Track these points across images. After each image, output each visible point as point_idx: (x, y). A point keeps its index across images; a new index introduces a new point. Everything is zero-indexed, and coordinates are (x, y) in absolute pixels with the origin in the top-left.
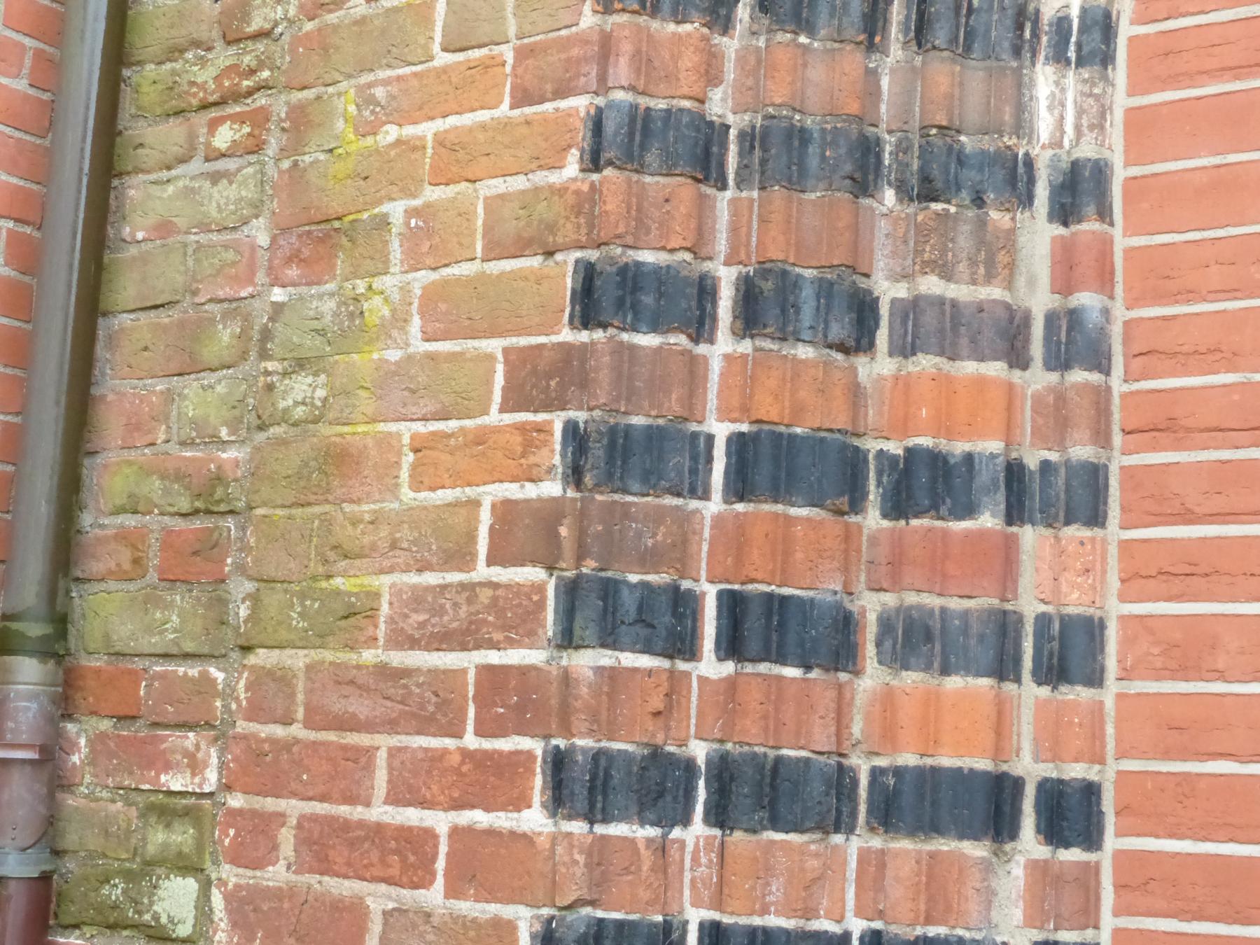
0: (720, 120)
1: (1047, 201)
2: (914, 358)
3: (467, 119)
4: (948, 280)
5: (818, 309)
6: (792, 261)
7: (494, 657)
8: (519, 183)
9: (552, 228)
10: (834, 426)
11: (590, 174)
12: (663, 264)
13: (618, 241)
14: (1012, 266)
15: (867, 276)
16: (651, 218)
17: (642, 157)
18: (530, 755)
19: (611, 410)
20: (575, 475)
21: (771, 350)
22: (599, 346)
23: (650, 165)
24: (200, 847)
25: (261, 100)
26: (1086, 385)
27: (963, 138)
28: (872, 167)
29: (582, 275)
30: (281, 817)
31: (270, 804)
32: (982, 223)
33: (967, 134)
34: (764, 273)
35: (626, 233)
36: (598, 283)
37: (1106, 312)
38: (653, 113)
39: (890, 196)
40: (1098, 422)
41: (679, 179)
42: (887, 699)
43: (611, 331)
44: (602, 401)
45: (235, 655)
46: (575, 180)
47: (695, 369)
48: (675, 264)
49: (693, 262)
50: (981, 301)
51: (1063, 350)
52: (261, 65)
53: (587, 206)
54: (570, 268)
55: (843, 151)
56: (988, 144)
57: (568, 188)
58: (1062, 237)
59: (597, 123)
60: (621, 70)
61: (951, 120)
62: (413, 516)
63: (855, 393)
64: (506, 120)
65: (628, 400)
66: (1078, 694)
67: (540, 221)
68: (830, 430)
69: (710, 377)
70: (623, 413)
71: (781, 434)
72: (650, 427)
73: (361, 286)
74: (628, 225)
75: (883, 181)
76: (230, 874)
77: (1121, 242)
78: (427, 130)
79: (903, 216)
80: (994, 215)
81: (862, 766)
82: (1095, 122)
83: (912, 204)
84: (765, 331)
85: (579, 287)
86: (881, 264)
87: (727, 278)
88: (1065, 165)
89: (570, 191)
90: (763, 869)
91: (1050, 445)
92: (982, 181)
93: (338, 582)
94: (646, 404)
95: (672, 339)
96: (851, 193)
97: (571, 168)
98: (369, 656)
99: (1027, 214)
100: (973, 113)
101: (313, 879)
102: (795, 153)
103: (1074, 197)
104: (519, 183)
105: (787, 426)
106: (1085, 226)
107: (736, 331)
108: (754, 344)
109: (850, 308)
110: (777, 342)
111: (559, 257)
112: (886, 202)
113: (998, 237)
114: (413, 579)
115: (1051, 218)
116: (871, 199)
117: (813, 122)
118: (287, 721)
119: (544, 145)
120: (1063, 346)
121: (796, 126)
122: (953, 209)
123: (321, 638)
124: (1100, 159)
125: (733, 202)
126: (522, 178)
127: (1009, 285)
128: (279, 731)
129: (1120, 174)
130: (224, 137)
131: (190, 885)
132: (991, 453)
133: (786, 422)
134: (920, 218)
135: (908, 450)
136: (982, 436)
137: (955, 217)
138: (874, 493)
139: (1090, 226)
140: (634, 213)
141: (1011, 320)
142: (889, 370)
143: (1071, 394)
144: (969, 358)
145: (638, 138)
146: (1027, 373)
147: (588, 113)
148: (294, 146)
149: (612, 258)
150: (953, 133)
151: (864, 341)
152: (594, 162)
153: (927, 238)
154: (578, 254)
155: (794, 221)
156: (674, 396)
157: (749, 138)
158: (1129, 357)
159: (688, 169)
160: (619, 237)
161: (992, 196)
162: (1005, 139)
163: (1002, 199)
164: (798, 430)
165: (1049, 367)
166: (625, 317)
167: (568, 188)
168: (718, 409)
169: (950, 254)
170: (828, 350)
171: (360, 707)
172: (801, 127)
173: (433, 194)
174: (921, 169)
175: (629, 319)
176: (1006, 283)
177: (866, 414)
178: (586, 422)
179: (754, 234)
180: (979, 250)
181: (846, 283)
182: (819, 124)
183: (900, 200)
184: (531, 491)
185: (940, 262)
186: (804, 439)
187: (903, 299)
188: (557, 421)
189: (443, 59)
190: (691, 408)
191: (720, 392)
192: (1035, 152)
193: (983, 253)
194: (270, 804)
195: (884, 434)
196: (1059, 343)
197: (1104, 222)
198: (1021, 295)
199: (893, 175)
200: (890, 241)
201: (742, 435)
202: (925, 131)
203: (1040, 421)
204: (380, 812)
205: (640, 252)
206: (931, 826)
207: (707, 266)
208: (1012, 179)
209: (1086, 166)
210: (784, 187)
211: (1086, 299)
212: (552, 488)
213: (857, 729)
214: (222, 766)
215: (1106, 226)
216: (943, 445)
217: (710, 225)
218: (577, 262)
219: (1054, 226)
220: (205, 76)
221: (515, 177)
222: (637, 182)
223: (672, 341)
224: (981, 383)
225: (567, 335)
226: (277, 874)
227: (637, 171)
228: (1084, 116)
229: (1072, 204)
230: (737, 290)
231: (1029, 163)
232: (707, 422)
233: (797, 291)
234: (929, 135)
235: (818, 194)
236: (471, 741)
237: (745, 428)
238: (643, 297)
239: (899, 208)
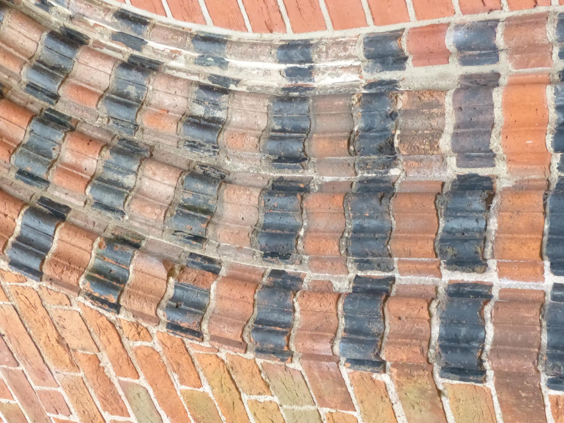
0: (352, 283)
1: (393, 72)
2: (494, 150)
4: (442, 132)
5: (465, 217)
6: (434, 236)
8: (398, 408)
9: (423, 392)
10: (542, 203)
11: (387, 367)
12: (440, 321)
13: (425, 352)
14: (431, 91)
15: (443, 184)
16: (412, 328)
17: (373, 335)
19: (538, 359)
21: (492, 248)
22: (494, 366)
23: (379, 330)
26: (505, 34)
27: (356, 129)
28: (376, 185)
29: (450, 374)
32: (406, 113)
33: (354, 126)
34: (443, 254)
35: (420, 346)
36: (453, 365)
37: (458, 27)
38: (347, 327)
39: (394, 172)
40: (530, 23)
41: (385, 311)
43: (484, 357)
44: (531, 365)
46: (391, 377)
48: (439, 314)
49: (438, 300)
50: (455, 109)
51: (485, 52)
53: (406, 370)
54: (447, 381)
55: (365, 205)
56: (358, 112)
57: (397, 381)
58: (413, 60)
59: (356, 362)
60: (323, 348)
61: (344, 138)
64: (362, 414)
65: (531, 346)
67: (420, 398)
68: (545, 205)
69: (514, 287)
70: (539, 349)
71: (549, 240)
72: (548, 331)
74: (415, 345)
75: (385, 177)
77: (413, 23)
79: (405, 163)
80: (400, 106)
82: (342, 47)
83: (398, 158)
84: (480, 252)
85: (458, 377)
86: (437, 175)
88: (370, 63)
89: (398, 380)
91: (549, 54)
92: (380, 115)
94: (533, 333)
95: (488, 315)
96: (390, 199)
97: (385, 378)
99: (401, 84)
100: (341, 124)
102: (368, 235)
103: (388, 56)
104: (398, 408)
105: (543, 235)
106: (404, 47)
107: (482, 270)
108: (489, 259)
109: (463, 196)
110: (487, 244)
111: (441, 387)
112: (398, 174)
113: (413, 102)
115: (403, 68)
116: (396, 184)
117: (350, 224)
119: (373, 393)
120: (482, 52)
121: (352, 235)
122: (398, 132)
124: (364, 42)
125: (401, 273)
126: (395, 407)
127: (444, 91)
129: (373, 29)
132: (555, 94)
133: (540, 237)
134: (405, 153)
135: (556, 151)
136: (543, 101)
137: (403, 130)
139: (404, 44)
140: (408, 341)
141: (467, 88)
142: (504, 166)
143: (512, 43)
144: (492, 114)
145: (362, 338)
146: (502, 73)
147: (350, 368)
149: (436, 356)
150: (352, 136)
151: (486, 184)
152: (380, 365)
153: (416, 147)
154: (437, 376)
155: (409, 235)
156: (526, 315)
157: (362, 264)
159: (379, 306)
160: (422, 351)
161: (389, 108)
162: (354, 103)
163: (390, 101)
164: (546, 227)
165: (496, 60)
166: (474, 348)
167: (397, 381)
168: (536, 281)
169: (426, 132)
170: (491, 209)
172: (352, 232)
174: (374, 154)
175: (476, 345)
176: (442, 94)
177: (535, 180)
178: (547, 375)
179: (420, 259)
180: (423, 113)
181: (446, 200)
182: (351, 220)
183: (396, 165)
185: (431, 138)
186: (552, 223)
187: (457, 160)
188: (549, 393)
190: (534, 302)
191: (524, 280)
192: (364, 83)
193: (424, 111)
195: (547, 167)
196: (479, 55)
197: (401, 35)
198: (451, 83)
199: (381, 171)
200: (421, 170)
201: (552, 266)
202: (352, 153)
203: (533, 61)
205: (433, 336)
207: (441, 290)
208: (378, 96)
209: (368, 50)
210: (388, 243)
215: (404, 33)
216: (551, 127)
217: (415, 289)
218: (442, 377)
219: (407, 65)
221: (395, 411)
222: (388, 338)
223: (489, 316)
224: (507, 105)
225: (490, 384)
227: (382, 338)
228: (340, 55)
229: (392, 56)
230: (456, 270)
231: (370, 85)
232: (545, 289)
233: (454, 231)
234: (355, 151)
235: (393, 219)
237: (547, 263)
238: (462, 335)
239: (400, 166)
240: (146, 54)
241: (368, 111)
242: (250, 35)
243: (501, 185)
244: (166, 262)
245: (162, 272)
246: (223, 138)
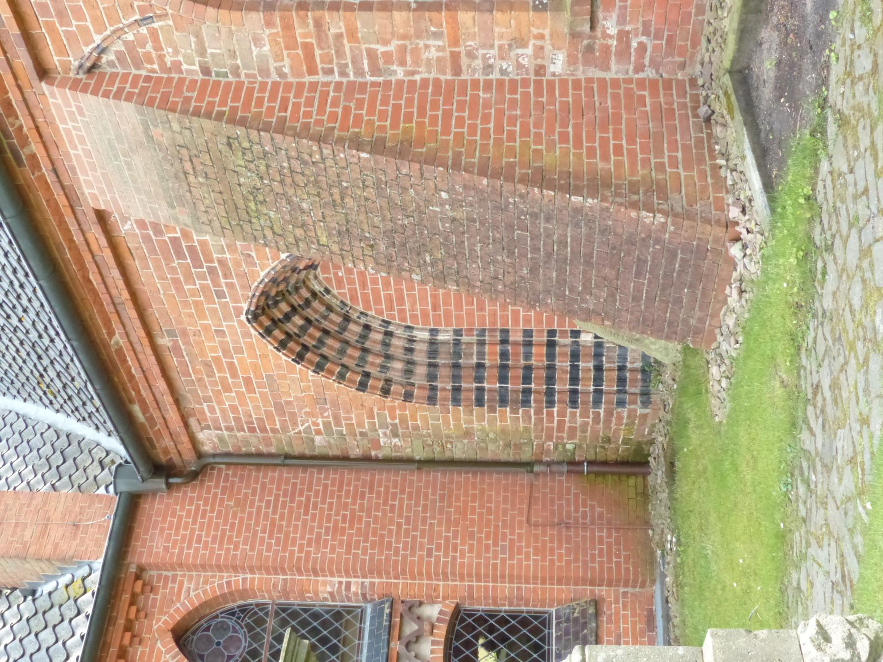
42: (536, 361)
47: (490, 390)
63: (491, 367)
66: (534, 334)
76: (565, 441)
77: (465, 327)
78: (452, 423)
81: (546, 363)
87: (475, 385)
90: (561, 379)
130: (449, 446)
148: (452, 438)
171: (540, 427)
211: (475, 333)
212: (508, 409)
213: (540, 364)
220: (438, 449)
226: (565, 435)
241: (454, 348)
242: (420, 326)
243: (487, 365)
244: (402, 385)
245: (401, 388)
246: (415, 353)
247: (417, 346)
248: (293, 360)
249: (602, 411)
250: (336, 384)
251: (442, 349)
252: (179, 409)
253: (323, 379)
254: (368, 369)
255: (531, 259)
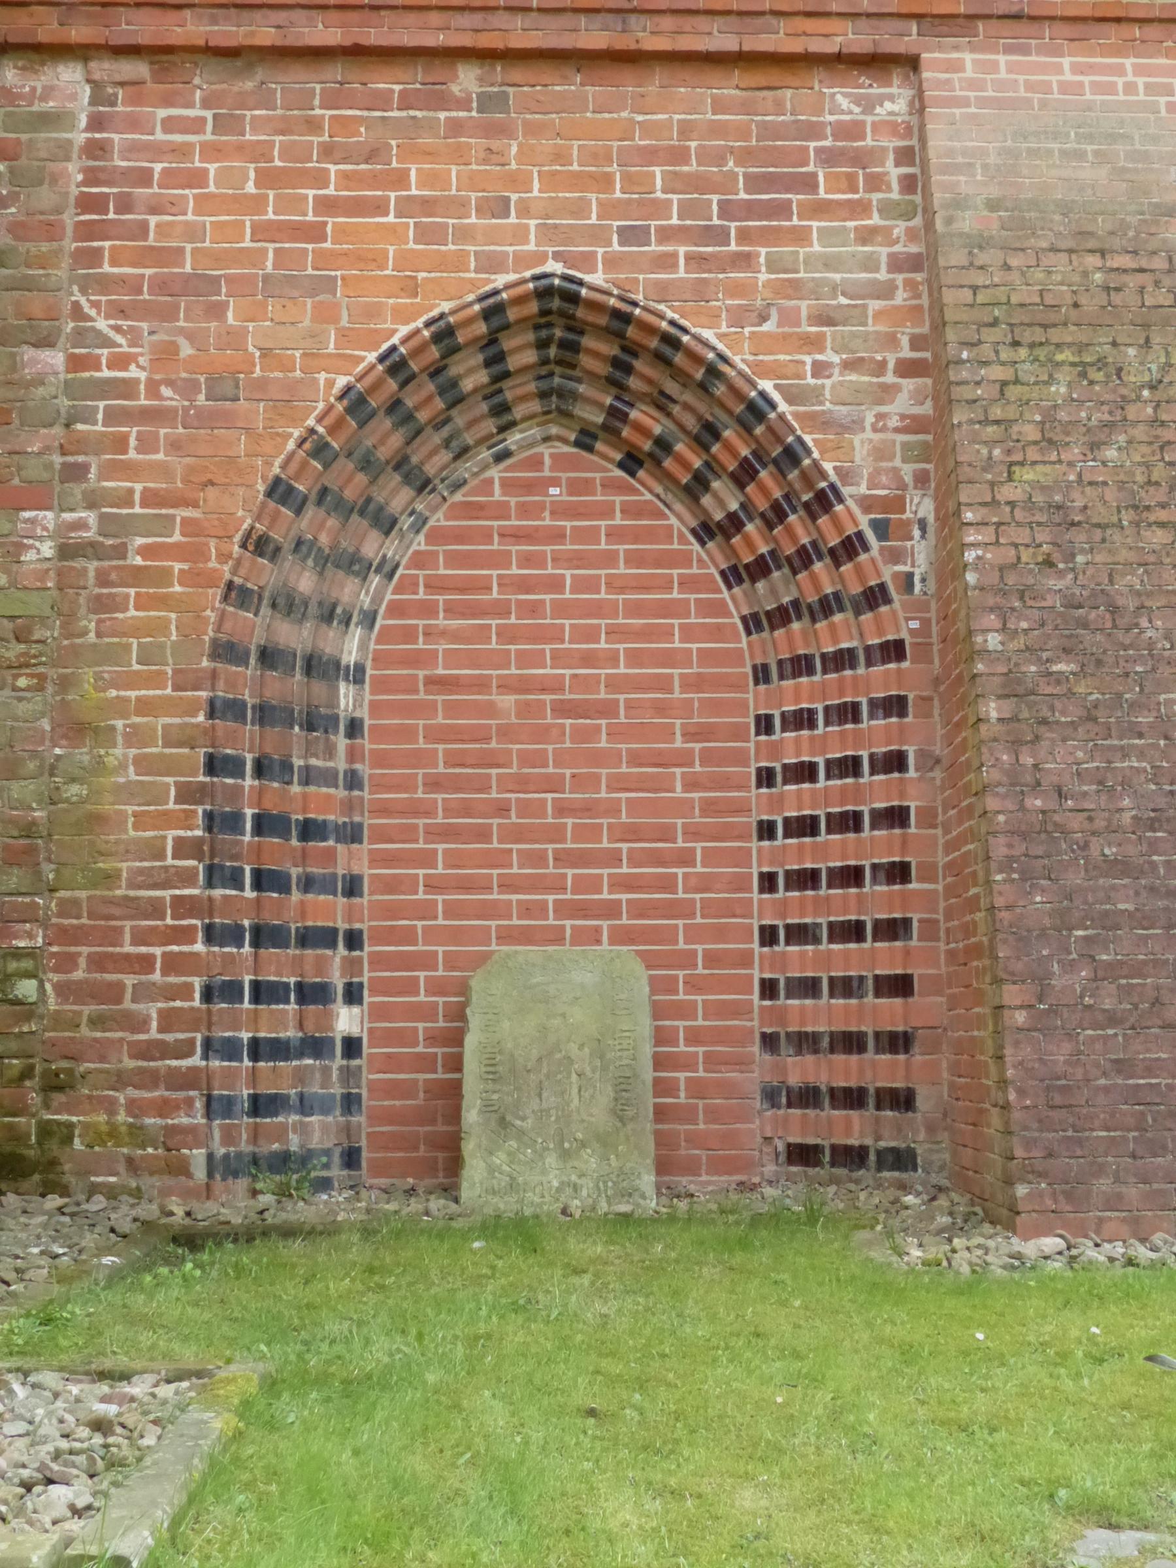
3: (151, 693)
7: (177, 892)
8: (177, 720)
18: (195, 926)
20: (209, 829)
24: (37, 968)
25: (42, 669)
30: (79, 954)
31: (73, 949)
39: (297, 728)
45: (47, 893)
52: (41, 655)
60: (221, 684)
62: (136, 841)
73: (102, 752)
76: (55, 977)
77: (368, 746)
78: (133, 694)
87: (249, 758)
93: (101, 865)
97: (201, 718)
98: (118, 892)
101: (98, 976)
104: (177, 720)
114: (138, 864)
118: (78, 917)
123: (94, 886)
128: (75, 922)
129: (367, 723)
130: (22, 682)
131: (33, 983)
138: (294, 833)
158: (371, 786)
171: (117, 911)
173: (138, 720)
184: (189, 833)
189: (136, 667)
194: (73, 949)
204: (128, 949)
206: (315, 946)
212: (199, 833)
214: (44, 937)
225: (201, 778)
236: (169, 921)
240: (372, 574)
247: (332, 633)
248: (394, 349)
249: (196, 1061)
250: (297, 433)
251: (319, 688)
252: (192, 50)
253: (321, 406)
254: (310, 511)
255: (1152, 863)
